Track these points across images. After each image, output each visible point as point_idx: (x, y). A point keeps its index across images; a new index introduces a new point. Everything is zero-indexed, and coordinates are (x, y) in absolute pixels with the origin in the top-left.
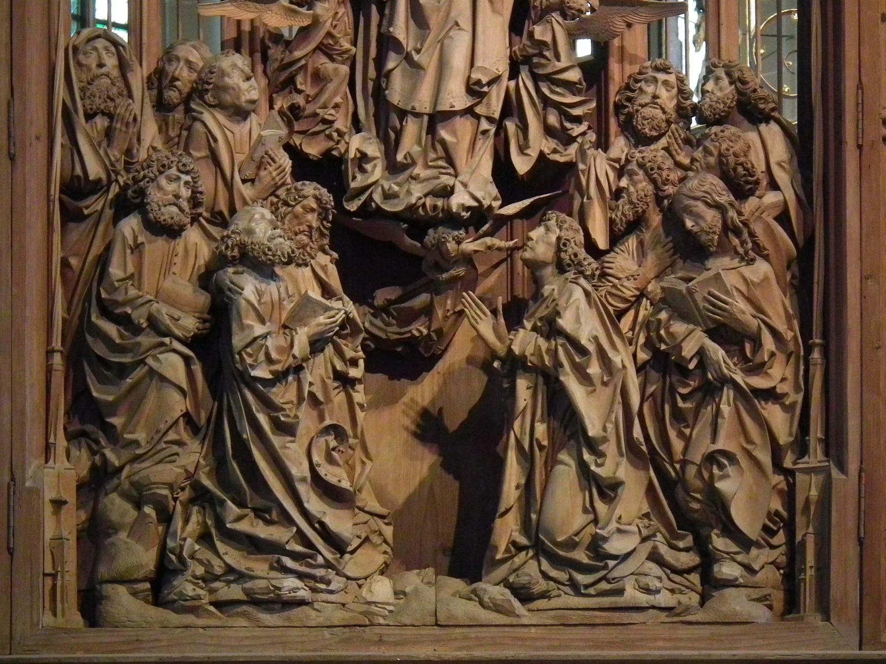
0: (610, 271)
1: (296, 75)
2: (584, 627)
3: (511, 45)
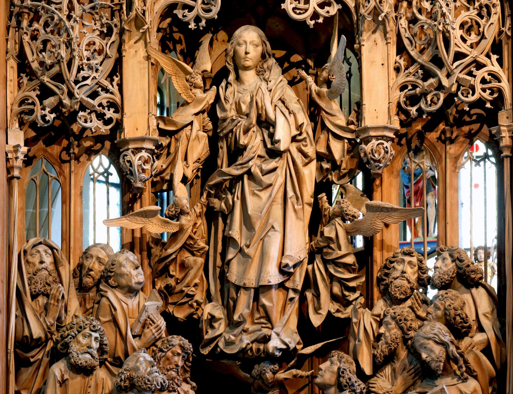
0: (373, 389)
1: (169, 265)
3: (311, 240)
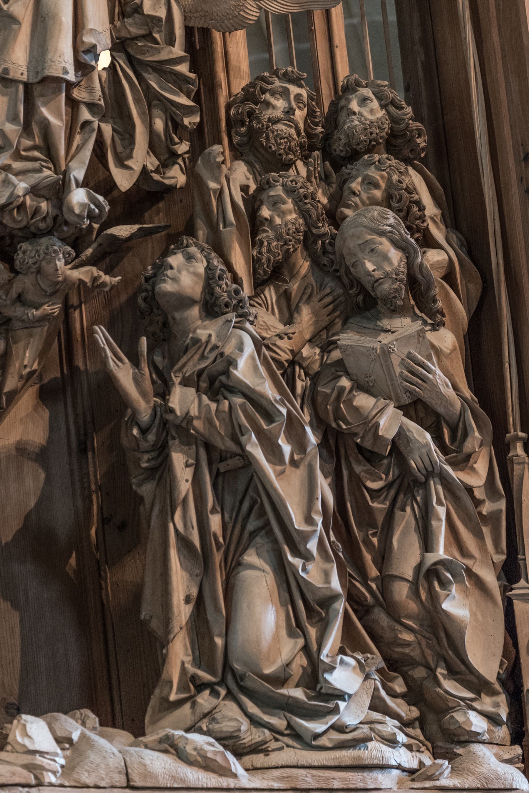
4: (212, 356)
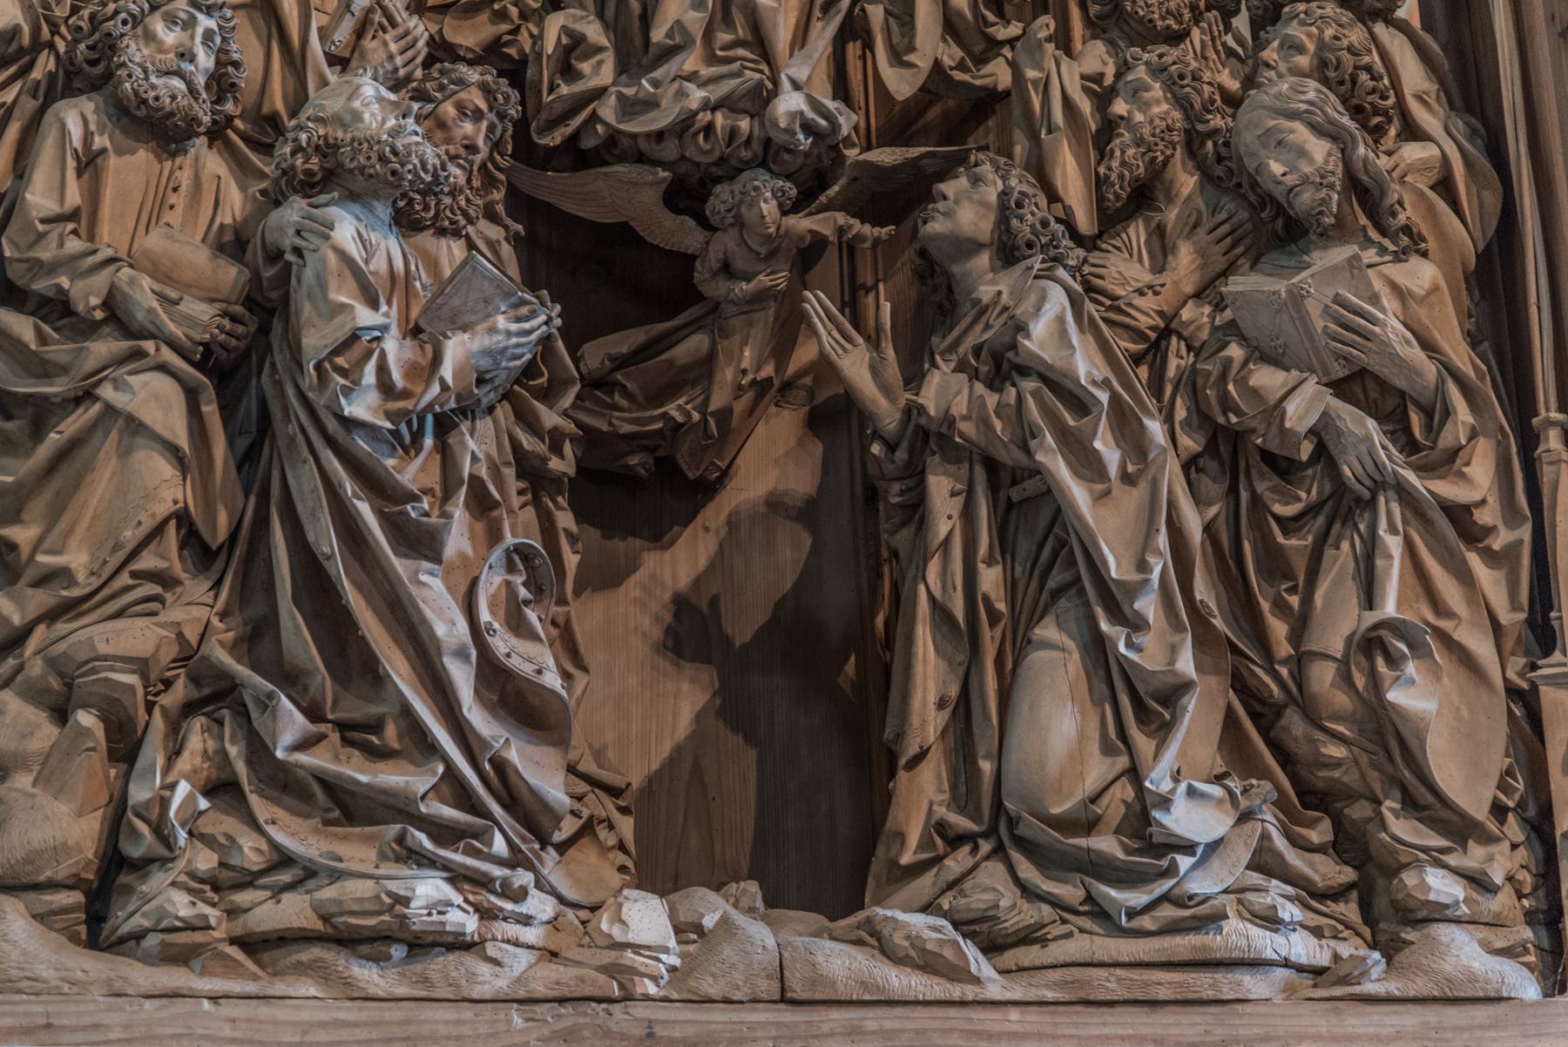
2: (1131, 1009)
4: (997, 324)
